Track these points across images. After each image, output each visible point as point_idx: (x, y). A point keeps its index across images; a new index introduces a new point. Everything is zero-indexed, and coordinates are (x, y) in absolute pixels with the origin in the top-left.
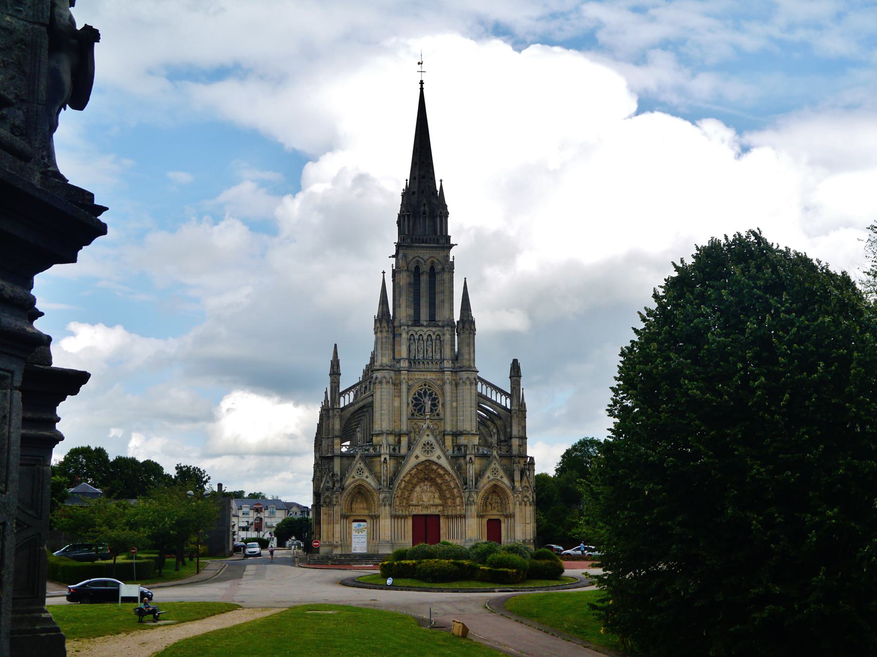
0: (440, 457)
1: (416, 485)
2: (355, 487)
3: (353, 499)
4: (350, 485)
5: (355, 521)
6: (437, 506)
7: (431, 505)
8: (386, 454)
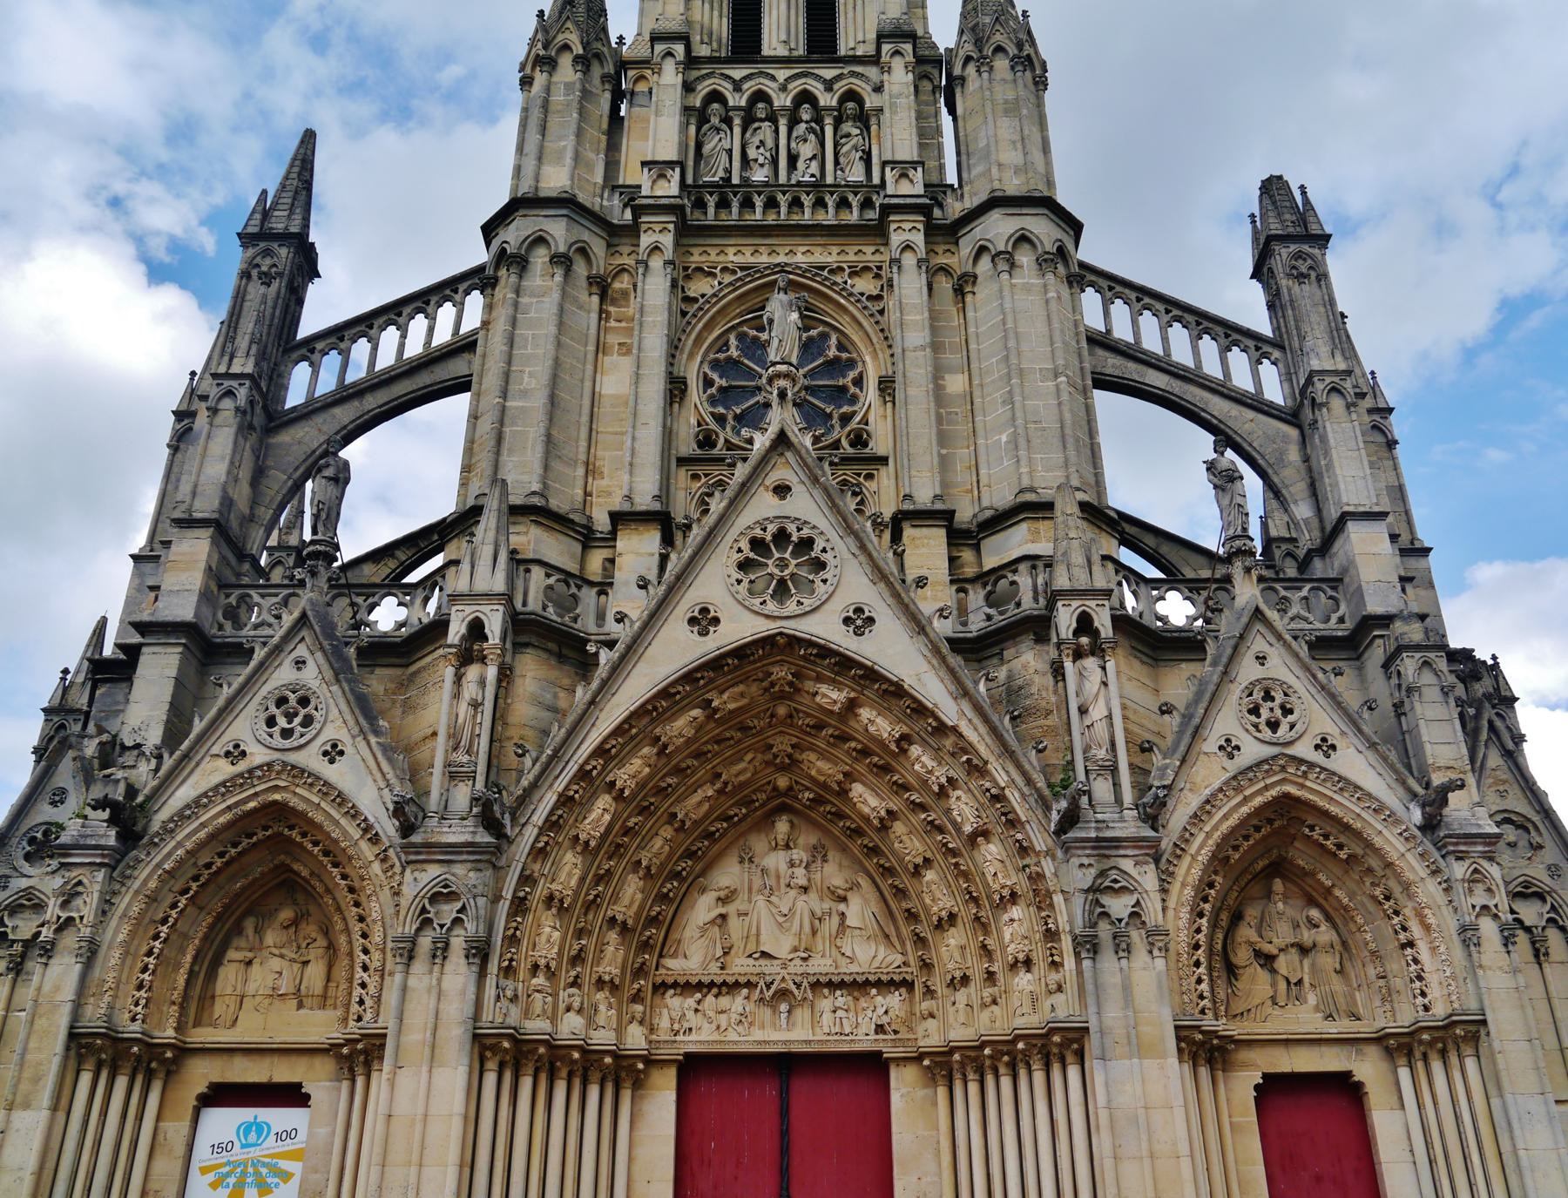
0: (871, 620)
1: (709, 835)
2: (242, 824)
3: (238, 930)
4: (197, 804)
5: (222, 1095)
6: (858, 986)
7: (816, 986)
8: (488, 596)
